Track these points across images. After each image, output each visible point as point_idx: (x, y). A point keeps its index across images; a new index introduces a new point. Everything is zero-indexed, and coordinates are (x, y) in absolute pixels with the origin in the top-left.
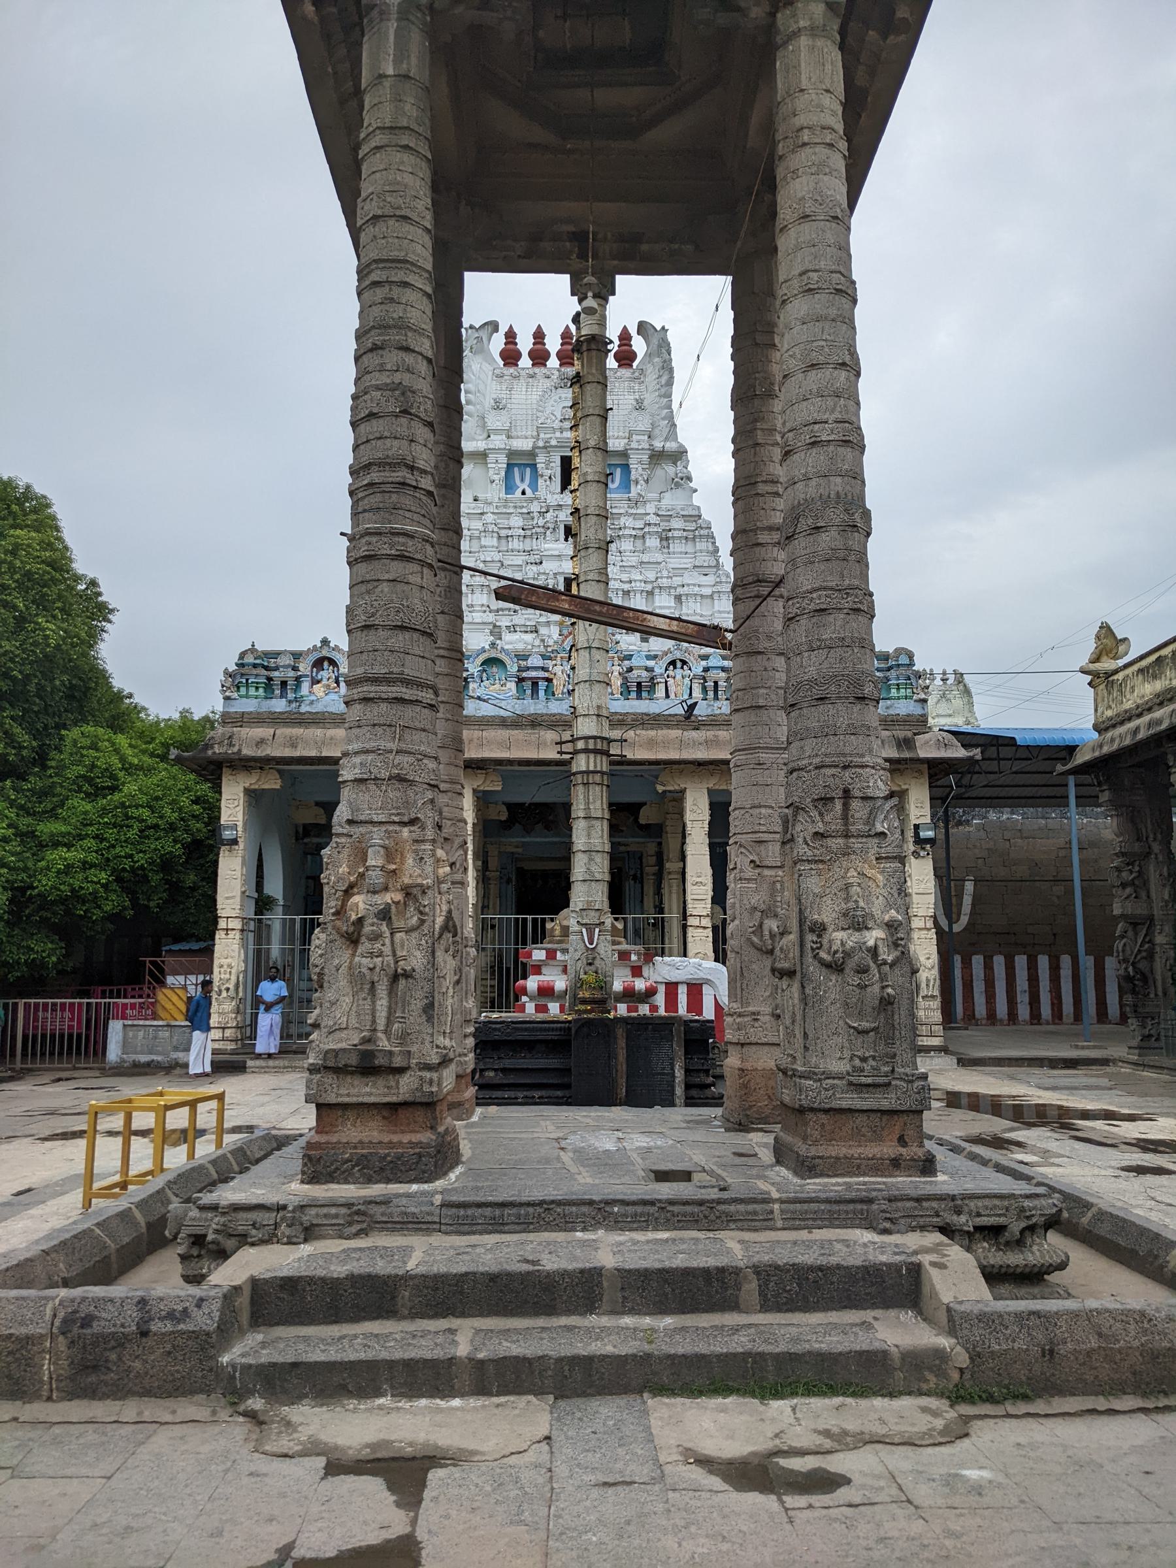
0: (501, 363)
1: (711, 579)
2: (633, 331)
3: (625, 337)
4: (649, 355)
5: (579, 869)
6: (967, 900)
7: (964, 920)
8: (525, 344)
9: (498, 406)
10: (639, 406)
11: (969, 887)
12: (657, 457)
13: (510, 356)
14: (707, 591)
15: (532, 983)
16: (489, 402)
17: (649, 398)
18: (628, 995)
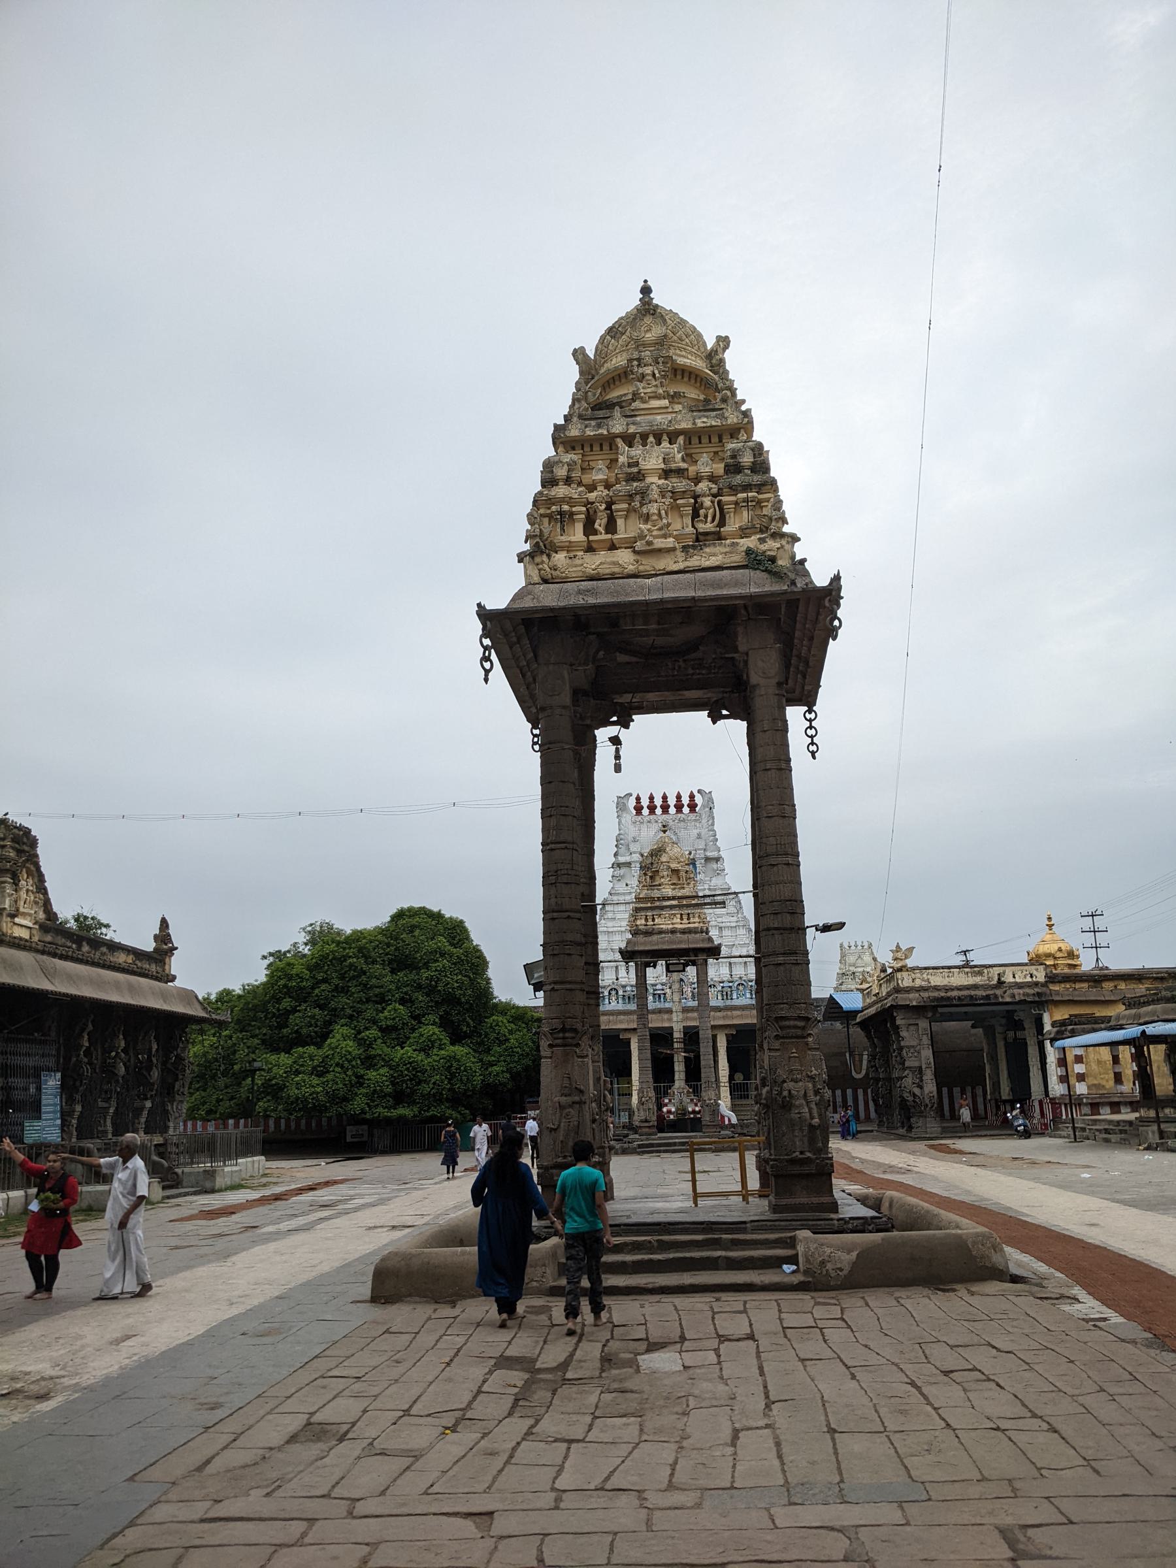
0: (634, 812)
1: (735, 919)
2: (696, 793)
3: (692, 796)
4: (703, 806)
5: (676, 1077)
6: (865, 1063)
7: (864, 1072)
8: (645, 802)
9: (635, 840)
10: (699, 836)
11: (865, 1057)
12: (708, 859)
13: (639, 809)
14: (734, 924)
15: (665, 1109)
16: (630, 838)
17: (704, 832)
18: (694, 1112)
